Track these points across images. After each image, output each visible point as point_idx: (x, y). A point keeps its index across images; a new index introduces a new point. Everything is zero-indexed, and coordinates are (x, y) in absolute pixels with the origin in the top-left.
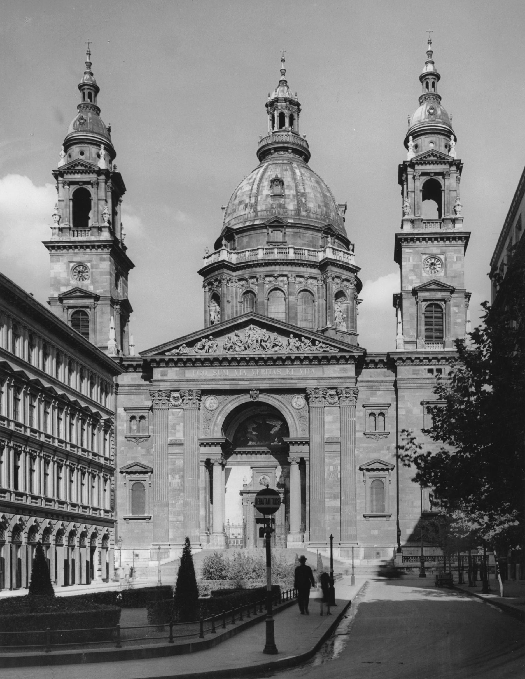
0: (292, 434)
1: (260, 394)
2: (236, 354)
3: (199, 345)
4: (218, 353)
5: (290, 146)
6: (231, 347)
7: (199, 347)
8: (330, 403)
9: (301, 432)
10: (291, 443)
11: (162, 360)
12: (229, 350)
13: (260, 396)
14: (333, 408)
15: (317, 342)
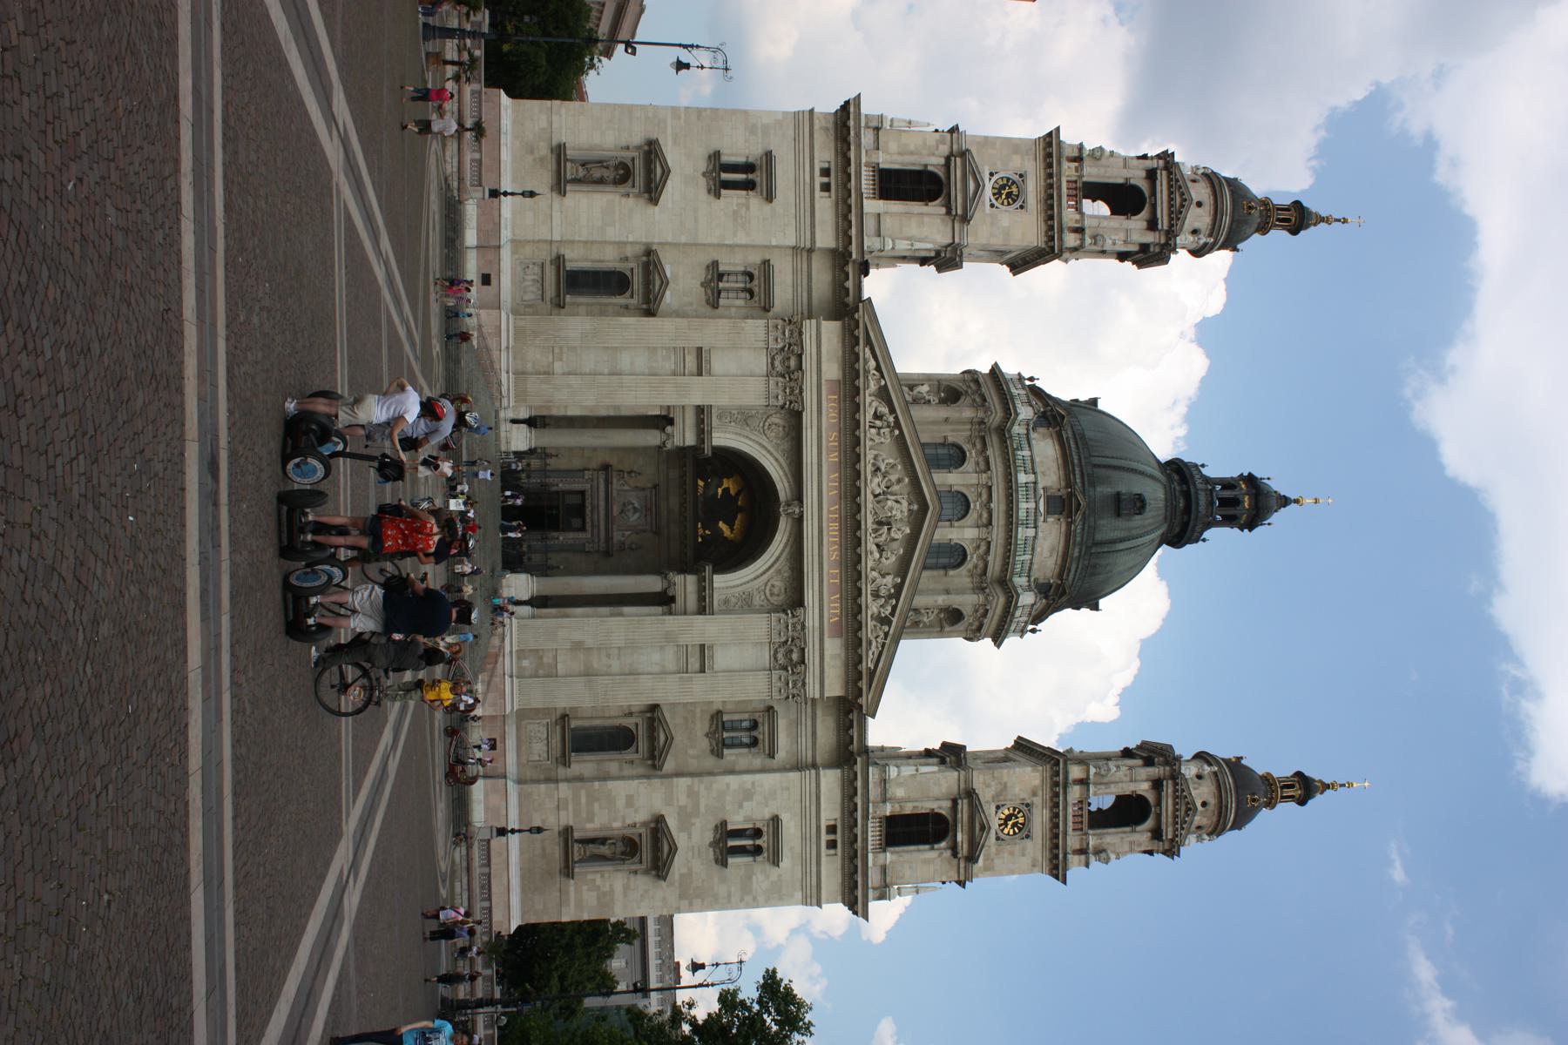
0: (720, 581)
1: (794, 518)
2: (866, 479)
3: (884, 410)
4: (869, 443)
5: (1193, 517)
6: (878, 469)
7: (879, 409)
8: (776, 652)
9: (724, 597)
10: (705, 581)
11: (857, 339)
12: (874, 465)
13: (790, 520)
14: (768, 657)
15: (886, 629)
